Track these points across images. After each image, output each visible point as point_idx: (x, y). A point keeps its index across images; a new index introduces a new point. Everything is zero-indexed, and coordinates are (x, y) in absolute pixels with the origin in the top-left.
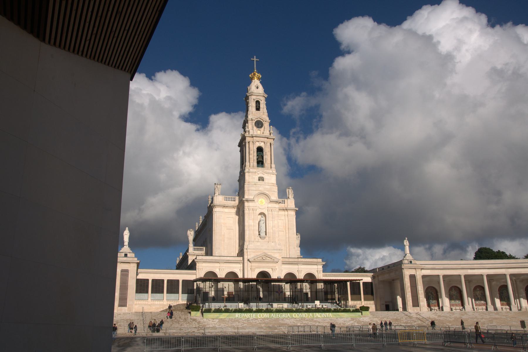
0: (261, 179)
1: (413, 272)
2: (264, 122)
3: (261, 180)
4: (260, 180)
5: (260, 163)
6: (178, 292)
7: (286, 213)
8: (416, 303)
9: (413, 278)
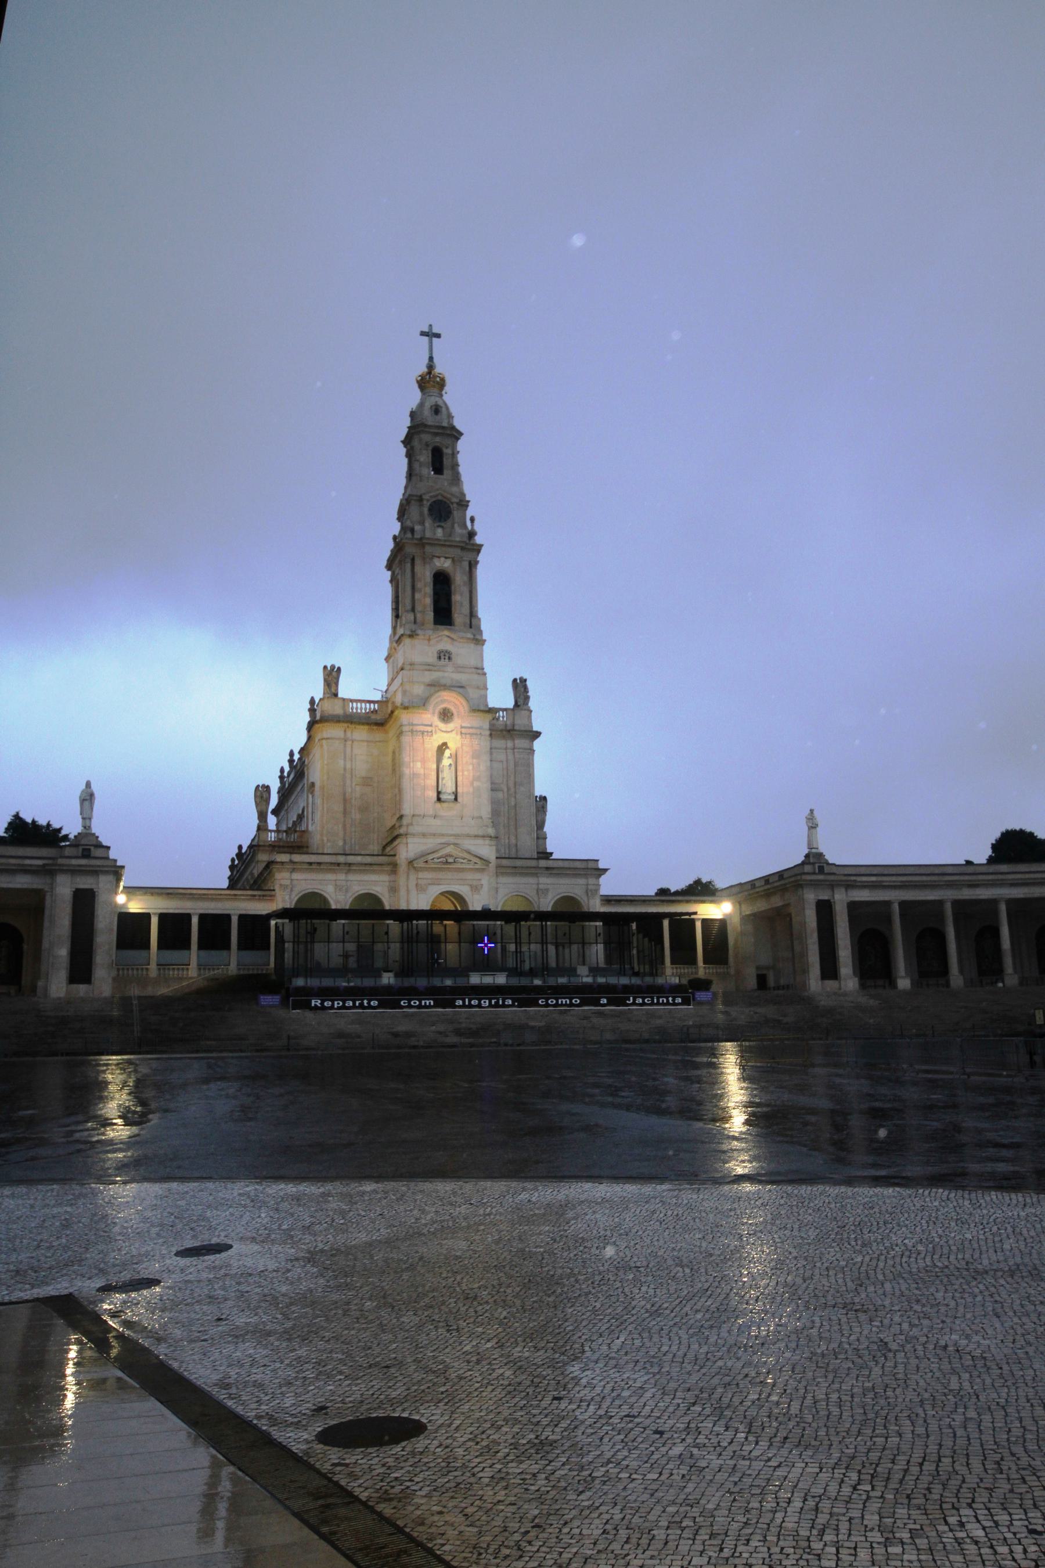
0: (444, 655)
1: (824, 896)
2: (455, 505)
4: (443, 657)
5: (443, 615)
6: (227, 946)
7: (510, 744)
8: (830, 970)
9: (825, 909)
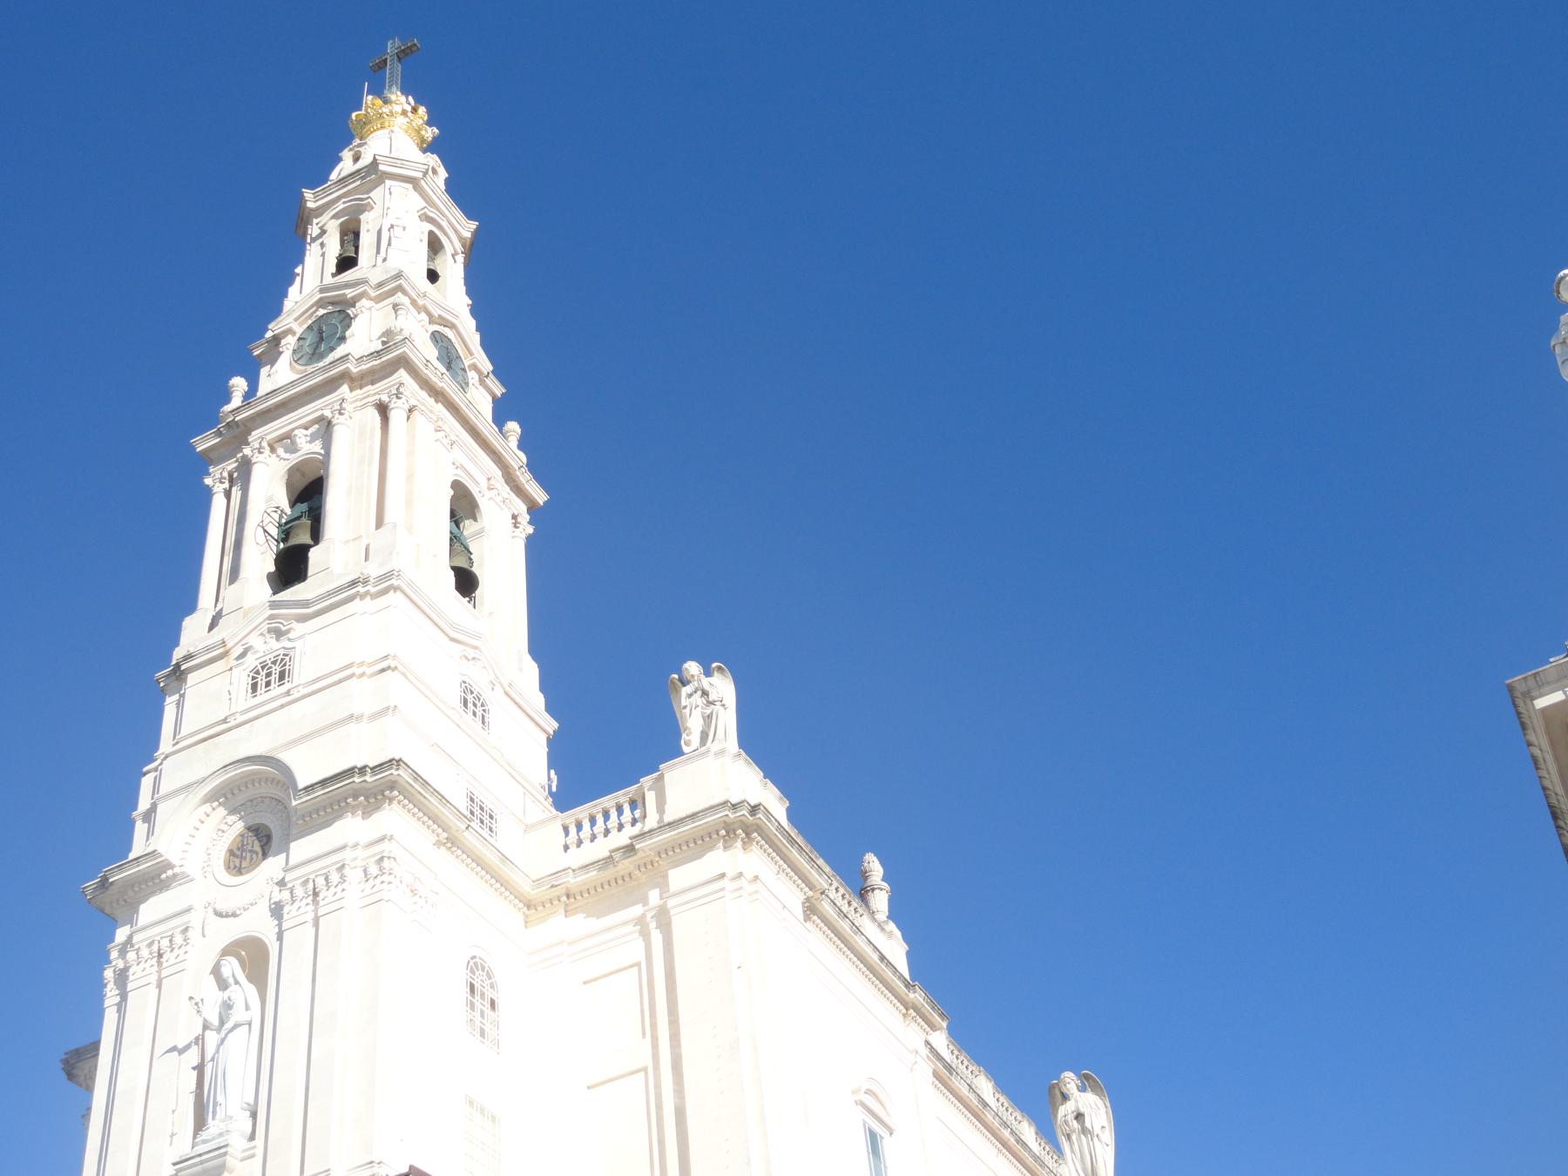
3: (474, 714)
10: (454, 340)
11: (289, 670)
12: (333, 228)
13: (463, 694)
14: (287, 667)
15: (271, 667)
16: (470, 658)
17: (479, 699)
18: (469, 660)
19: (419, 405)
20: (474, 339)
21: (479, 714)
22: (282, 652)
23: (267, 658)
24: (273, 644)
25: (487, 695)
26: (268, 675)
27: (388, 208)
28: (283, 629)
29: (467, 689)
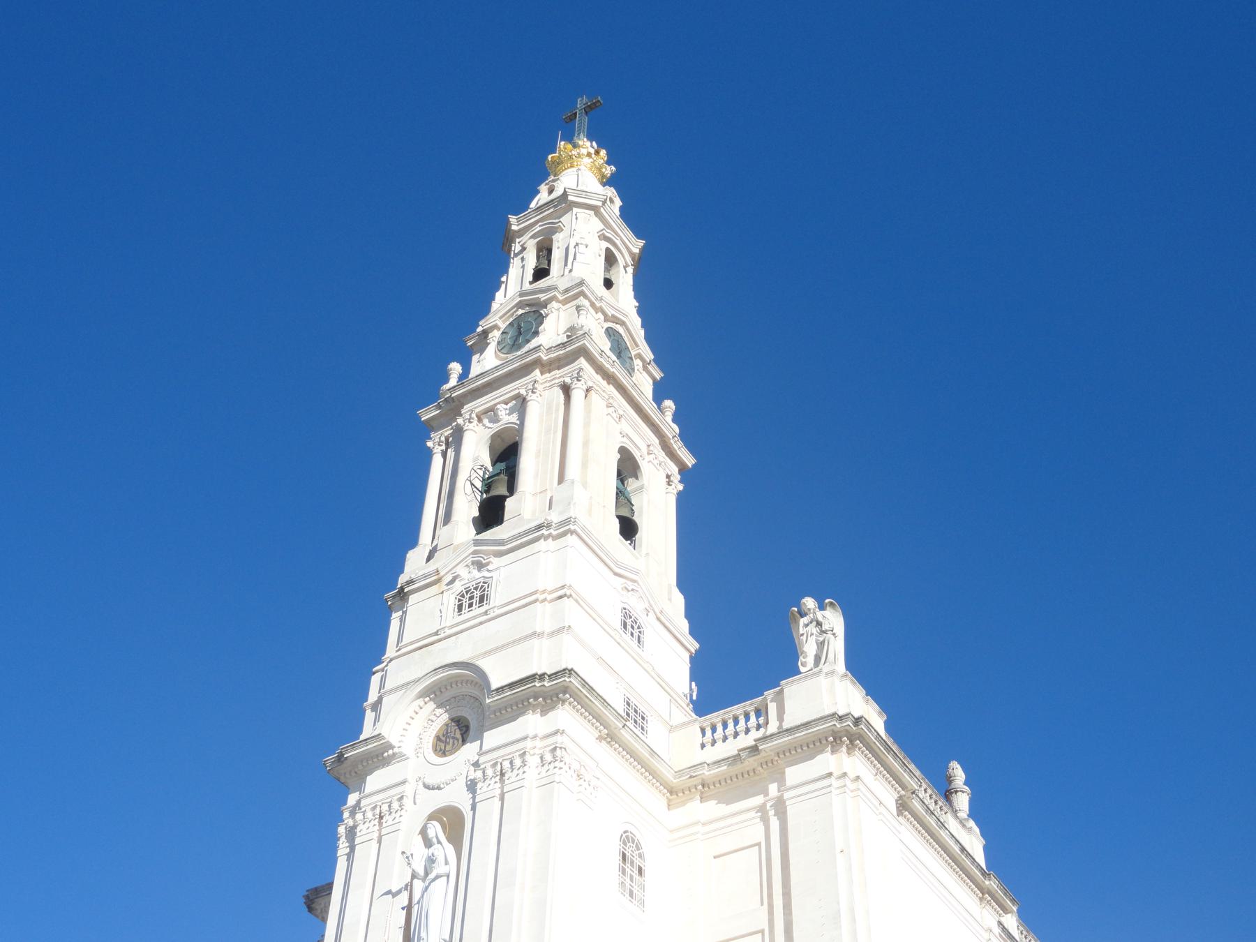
3: (632, 634)
10: (623, 334)
11: (487, 595)
12: (531, 246)
13: (623, 618)
14: (486, 592)
15: (473, 592)
16: (630, 589)
17: (636, 623)
18: (629, 591)
19: (594, 386)
20: (640, 333)
21: (636, 635)
22: (482, 580)
23: (470, 585)
24: (476, 574)
25: (642, 619)
26: (471, 598)
27: (574, 230)
28: (484, 562)
29: (626, 614)
